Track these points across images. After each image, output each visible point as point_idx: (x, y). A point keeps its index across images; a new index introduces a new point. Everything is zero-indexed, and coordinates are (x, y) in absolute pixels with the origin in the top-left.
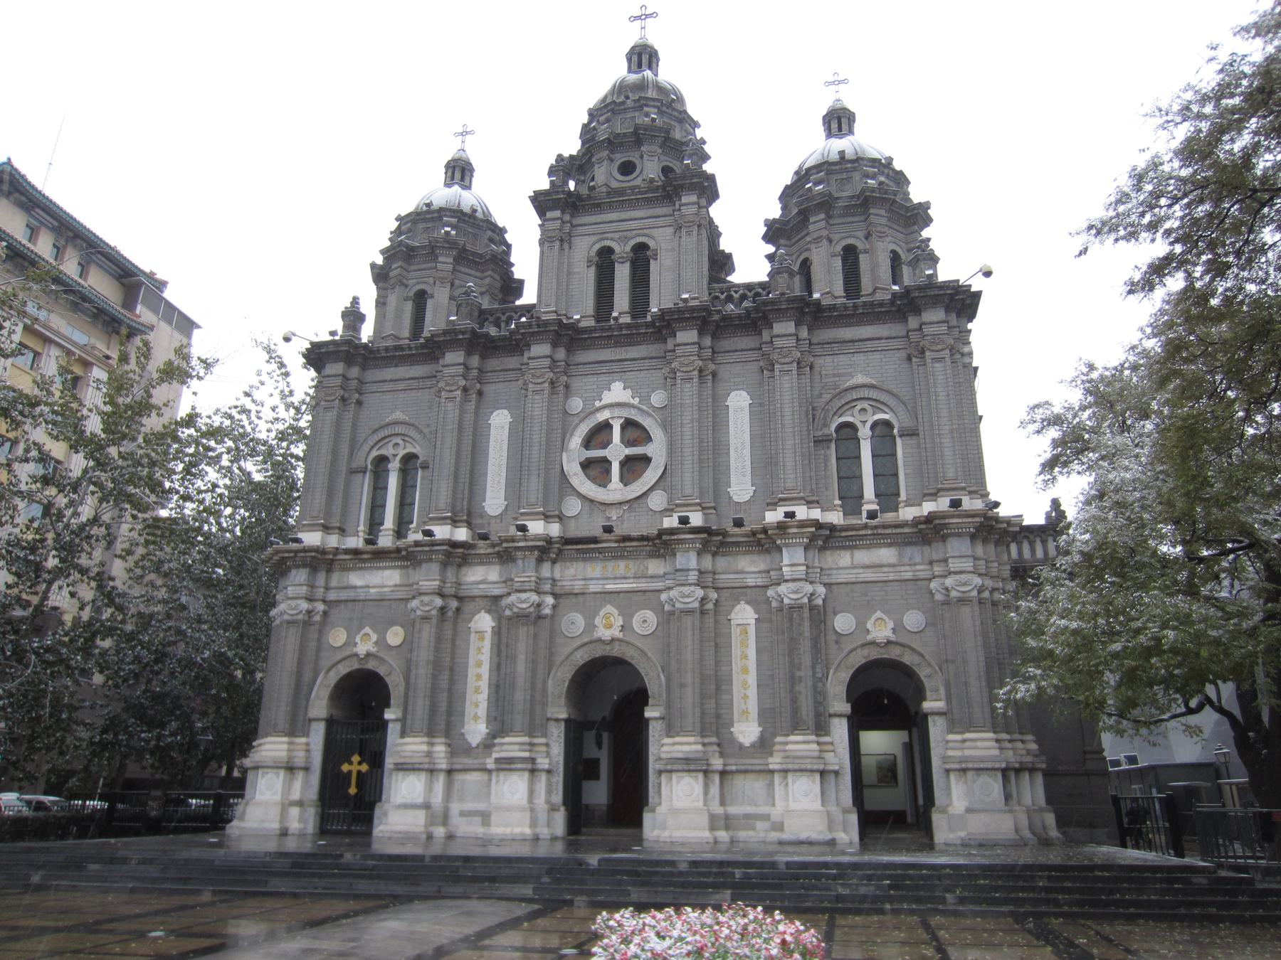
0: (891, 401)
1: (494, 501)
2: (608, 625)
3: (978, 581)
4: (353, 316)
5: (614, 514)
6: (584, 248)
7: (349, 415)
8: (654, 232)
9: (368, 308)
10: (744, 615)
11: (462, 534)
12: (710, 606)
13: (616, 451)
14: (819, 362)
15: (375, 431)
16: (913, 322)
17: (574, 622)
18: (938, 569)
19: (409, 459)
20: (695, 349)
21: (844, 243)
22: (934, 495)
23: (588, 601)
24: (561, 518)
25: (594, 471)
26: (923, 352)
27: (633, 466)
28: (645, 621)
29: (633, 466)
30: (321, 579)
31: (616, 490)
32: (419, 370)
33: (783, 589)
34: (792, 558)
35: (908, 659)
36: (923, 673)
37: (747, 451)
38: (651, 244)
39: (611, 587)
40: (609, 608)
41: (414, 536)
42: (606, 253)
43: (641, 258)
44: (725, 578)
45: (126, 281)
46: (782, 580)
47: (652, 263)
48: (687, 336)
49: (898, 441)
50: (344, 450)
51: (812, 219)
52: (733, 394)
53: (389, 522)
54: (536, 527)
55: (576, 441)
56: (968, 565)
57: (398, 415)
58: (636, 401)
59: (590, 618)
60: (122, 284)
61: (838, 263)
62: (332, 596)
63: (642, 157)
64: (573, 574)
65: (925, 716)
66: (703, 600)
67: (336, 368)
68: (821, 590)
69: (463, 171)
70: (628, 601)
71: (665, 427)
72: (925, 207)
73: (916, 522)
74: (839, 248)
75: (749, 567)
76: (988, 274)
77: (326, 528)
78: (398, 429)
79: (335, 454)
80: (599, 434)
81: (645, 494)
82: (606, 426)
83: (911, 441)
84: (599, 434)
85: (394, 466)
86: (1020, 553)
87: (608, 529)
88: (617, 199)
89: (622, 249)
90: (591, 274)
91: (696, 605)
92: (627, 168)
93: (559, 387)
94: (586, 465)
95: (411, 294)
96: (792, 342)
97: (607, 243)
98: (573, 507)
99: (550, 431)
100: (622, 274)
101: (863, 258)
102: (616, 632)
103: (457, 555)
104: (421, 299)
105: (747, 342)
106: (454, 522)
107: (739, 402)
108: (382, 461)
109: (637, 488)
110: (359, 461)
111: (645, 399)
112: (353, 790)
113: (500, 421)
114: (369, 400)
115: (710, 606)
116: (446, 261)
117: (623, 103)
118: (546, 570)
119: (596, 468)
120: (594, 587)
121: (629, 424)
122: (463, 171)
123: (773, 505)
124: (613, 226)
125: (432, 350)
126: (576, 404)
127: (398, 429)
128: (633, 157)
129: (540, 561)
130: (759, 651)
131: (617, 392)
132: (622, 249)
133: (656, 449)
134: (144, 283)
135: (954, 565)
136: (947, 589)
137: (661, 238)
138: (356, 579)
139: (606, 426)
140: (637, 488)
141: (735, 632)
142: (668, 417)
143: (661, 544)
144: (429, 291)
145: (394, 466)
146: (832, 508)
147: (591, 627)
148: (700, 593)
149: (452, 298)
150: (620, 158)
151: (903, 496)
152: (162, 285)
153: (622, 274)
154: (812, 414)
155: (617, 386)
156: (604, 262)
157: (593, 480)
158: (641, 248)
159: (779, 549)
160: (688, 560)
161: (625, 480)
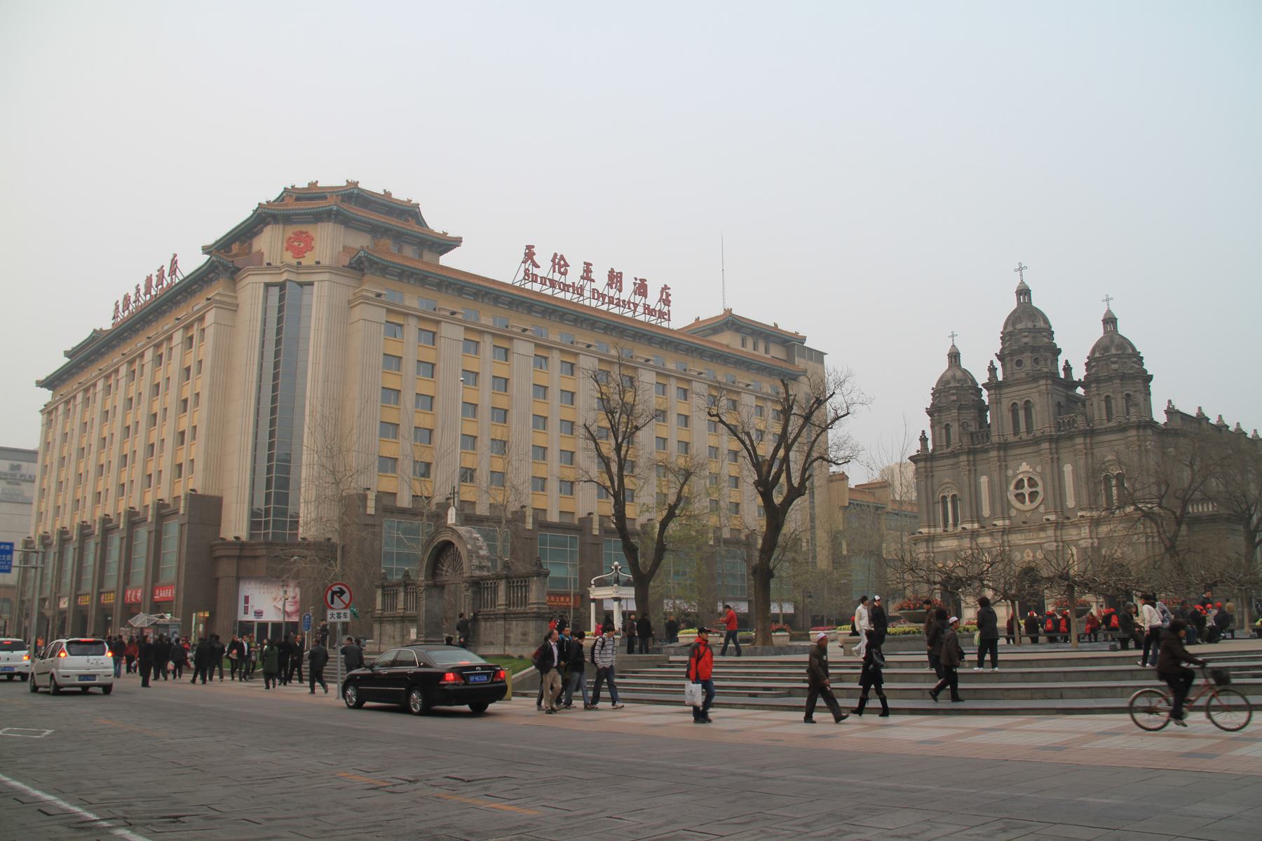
1: (986, 512)
2: (1028, 556)
4: (923, 439)
5: (1028, 515)
7: (929, 482)
9: (929, 435)
11: (976, 526)
12: (1060, 548)
13: (1027, 490)
15: (940, 486)
17: (1017, 556)
19: (954, 496)
20: (1048, 451)
21: (1105, 395)
23: (1021, 548)
24: (1010, 518)
25: (1020, 497)
27: (1033, 495)
28: (1039, 555)
29: (1033, 495)
30: (930, 544)
31: (1028, 505)
32: (951, 461)
37: (1072, 488)
38: (1032, 401)
39: (1028, 542)
40: (1028, 550)
41: (959, 528)
43: (1028, 406)
44: (1065, 538)
45: (787, 344)
47: (1033, 409)
48: (1045, 445)
50: (930, 495)
52: (1066, 466)
53: (951, 521)
54: (999, 523)
55: (1012, 487)
57: (947, 480)
58: (1031, 470)
59: (1022, 553)
60: (785, 347)
61: (1103, 404)
62: (935, 550)
64: (1016, 539)
66: (1057, 546)
67: (922, 464)
68: (1096, 540)
69: (955, 357)
70: (1033, 547)
71: (1042, 479)
74: (1103, 398)
77: (929, 526)
78: (948, 485)
79: (927, 500)
80: (1019, 484)
81: (1038, 507)
82: (1022, 480)
84: (1019, 484)
85: (949, 499)
86: (1203, 509)
87: (1025, 523)
88: (1018, 383)
90: (1010, 413)
91: (1054, 549)
92: (1019, 363)
93: (1003, 467)
94: (1017, 496)
95: (943, 426)
96: (1082, 446)
97: (1014, 401)
98: (1013, 513)
99: (1001, 485)
100: (1022, 413)
101: (1113, 401)
102: (1031, 558)
103: (974, 535)
104: (947, 427)
106: (972, 522)
108: (944, 498)
109: (1035, 504)
110: (936, 500)
111: (1035, 470)
113: (984, 480)
114: (936, 474)
115: (1060, 548)
116: (954, 412)
118: (1005, 538)
119: (1020, 497)
120: (1023, 543)
121: (1030, 479)
122: (955, 357)
124: (1015, 394)
125: (954, 455)
126: (1010, 472)
127: (948, 485)
129: (1002, 535)
131: (1024, 467)
132: (1020, 403)
133: (1039, 489)
134: (794, 344)
137: (1035, 398)
138: (943, 544)
139: (1022, 480)
140: (1035, 504)
144: (951, 424)
145: (949, 499)
147: (1022, 557)
149: (959, 426)
150: (1016, 358)
152: (803, 339)
153: (1022, 413)
155: (1024, 464)
157: (1019, 500)
160: (1050, 532)
161: (1031, 501)
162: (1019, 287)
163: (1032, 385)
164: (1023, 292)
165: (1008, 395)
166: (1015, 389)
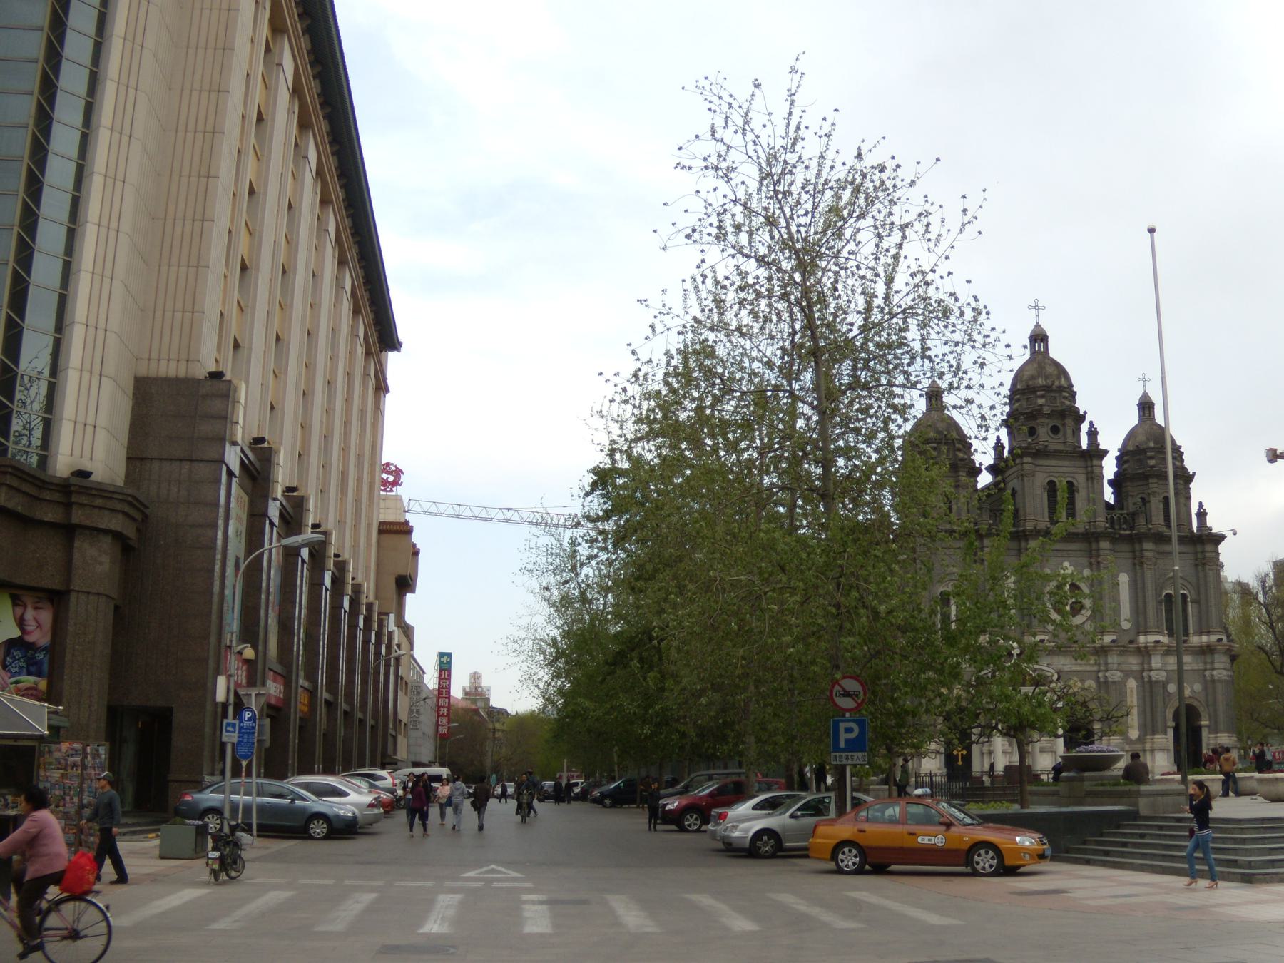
0: (1189, 586)
3: (1225, 673)
6: (1041, 480)
8: (1076, 476)
10: (1132, 684)
14: (1159, 561)
16: (1199, 548)
18: (1208, 667)
22: (1208, 633)
26: (1204, 564)
33: (1152, 673)
34: (1156, 661)
35: (1195, 703)
36: (1201, 709)
38: (1075, 482)
42: (1052, 484)
44: (1125, 667)
46: (1150, 670)
48: (1104, 545)
49: (1190, 604)
51: (1151, 481)
56: (1221, 666)
61: (1161, 506)
63: (1064, 425)
65: (1200, 728)
68: (1164, 674)
70: (1082, 676)
72: (1194, 473)
73: (1201, 647)
74: (1161, 498)
75: (1133, 662)
76: (1235, 534)
81: (1083, 623)
83: (1195, 605)
89: (1062, 483)
90: (1045, 496)
97: (1052, 478)
105: (1125, 547)
107: (1124, 578)
112: (960, 763)
117: (1051, 387)
123: (1146, 633)
128: (1058, 423)
130: (1138, 699)
131: (1068, 568)
135: (1217, 665)
136: (1212, 675)
137: (1080, 480)
141: (1128, 691)
142: (1095, 583)
143: (1103, 651)
146: (1163, 635)
148: (1119, 674)
150: (1052, 423)
151: (1191, 630)
154: (1159, 588)
156: (1052, 488)
158: (1070, 484)
159: (1150, 656)
160: (1113, 659)
162: (1033, 331)
163: (1078, 463)
164: (1039, 338)
165: (1044, 468)
166: (1053, 462)
